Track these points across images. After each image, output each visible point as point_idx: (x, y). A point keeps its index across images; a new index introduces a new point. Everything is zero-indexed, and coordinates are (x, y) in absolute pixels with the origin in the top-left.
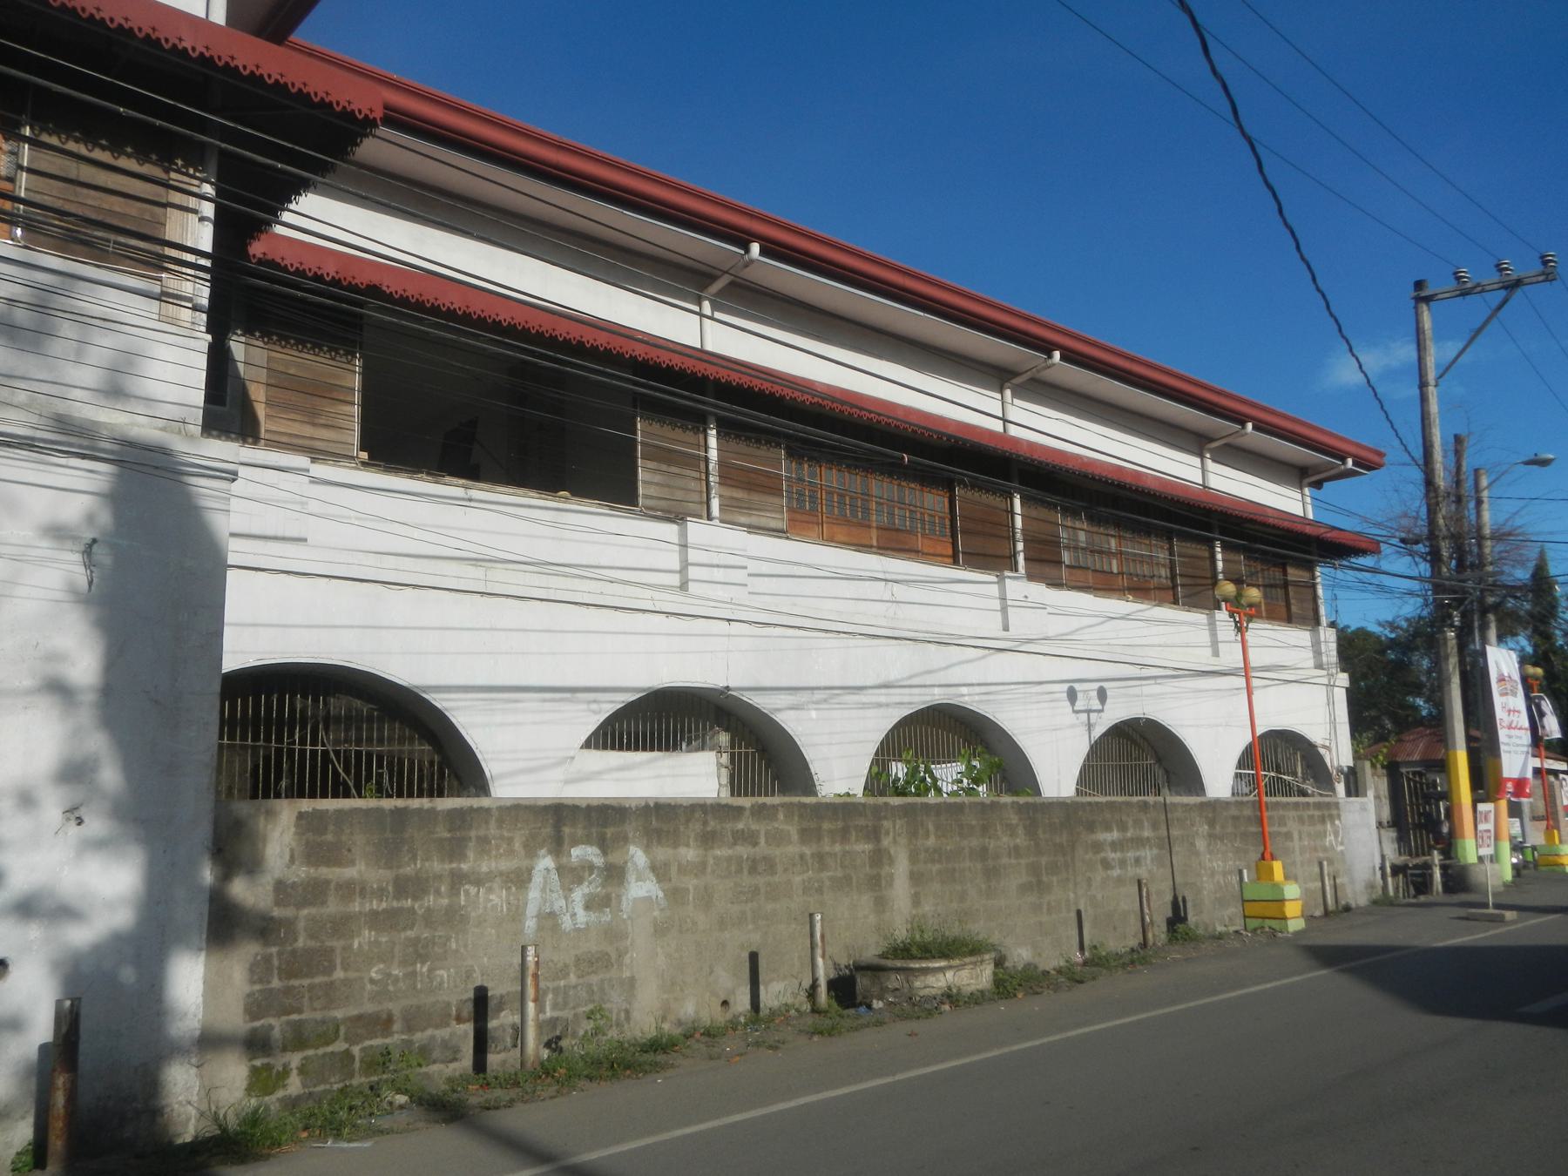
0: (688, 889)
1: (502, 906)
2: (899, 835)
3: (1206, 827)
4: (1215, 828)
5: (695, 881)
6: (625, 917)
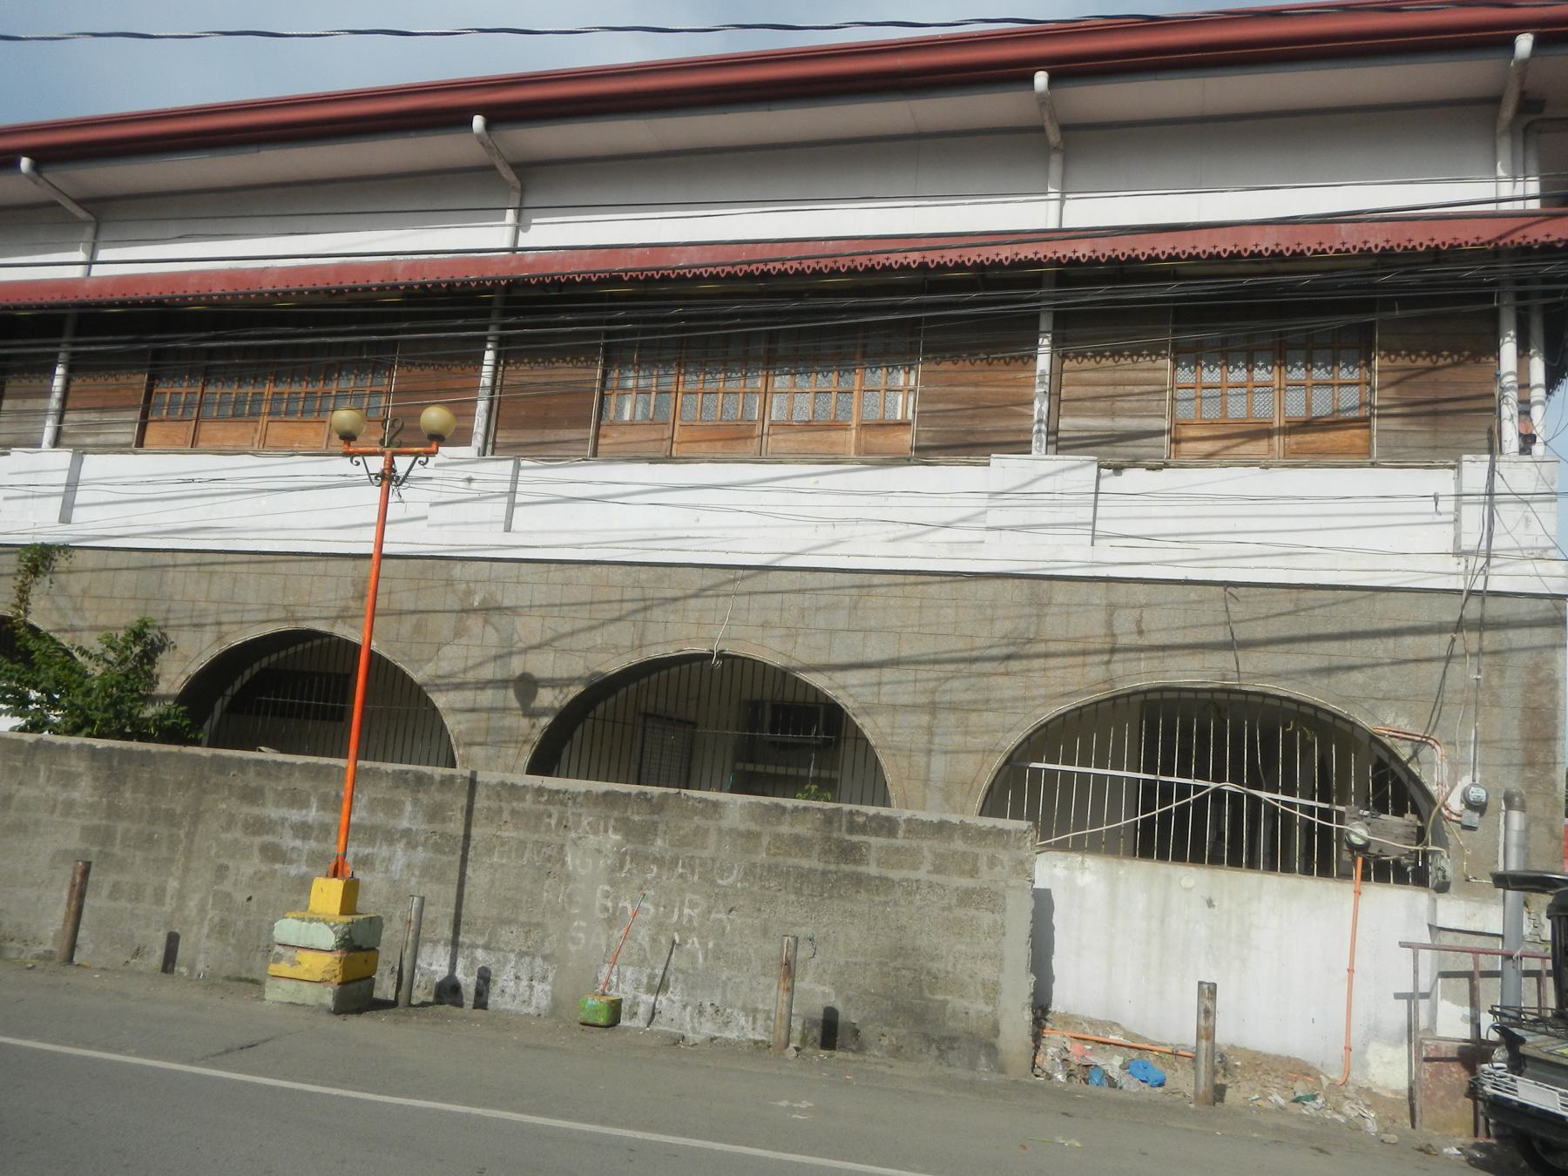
3: (616, 837)
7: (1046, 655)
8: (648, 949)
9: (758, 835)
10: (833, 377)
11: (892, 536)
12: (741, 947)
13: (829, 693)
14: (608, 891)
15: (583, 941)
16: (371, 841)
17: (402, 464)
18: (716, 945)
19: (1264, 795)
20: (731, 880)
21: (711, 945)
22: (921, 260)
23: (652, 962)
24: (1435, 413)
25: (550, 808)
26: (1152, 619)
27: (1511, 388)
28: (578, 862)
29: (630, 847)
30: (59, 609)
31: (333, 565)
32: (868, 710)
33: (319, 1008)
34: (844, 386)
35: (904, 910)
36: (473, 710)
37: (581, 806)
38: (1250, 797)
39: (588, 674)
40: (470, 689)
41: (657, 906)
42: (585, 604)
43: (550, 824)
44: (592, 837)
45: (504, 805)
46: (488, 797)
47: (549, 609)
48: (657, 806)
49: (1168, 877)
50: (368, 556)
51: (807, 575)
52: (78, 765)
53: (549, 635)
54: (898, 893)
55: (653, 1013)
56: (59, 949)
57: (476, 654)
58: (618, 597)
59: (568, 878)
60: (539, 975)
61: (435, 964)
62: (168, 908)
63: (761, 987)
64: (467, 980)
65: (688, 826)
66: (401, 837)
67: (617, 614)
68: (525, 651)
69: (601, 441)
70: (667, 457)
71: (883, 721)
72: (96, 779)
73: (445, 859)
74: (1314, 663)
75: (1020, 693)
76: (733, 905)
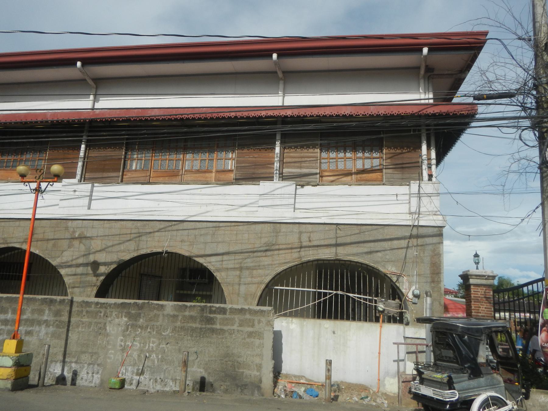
7: (279, 250)
8: (137, 360)
9: (177, 316)
10: (207, 154)
11: (227, 209)
12: (171, 357)
13: (205, 264)
14: (122, 339)
15: (113, 358)
16: (32, 325)
17: (43, 185)
18: (162, 357)
19: (351, 295)
20: (167, 333)
21: (160, 357)
22: (235, 115)
23: (138, 364)
24: (403, 168)
25: (101, 310)
26: (314, 236)
27: (425, 160)
28: (111, 329)
29: (131, 322)
31: (22, 223)
32: (218, 270)
33: (6, 389)
34: (210, 158)
35: (229, 340)
36: (75, 275)
37: (113, 308)
38: (347, 296)
39: (118, 260)
40: (74, 267)
41: (140, 343)
42: (118, 235)
43: (101, 316)
44: (116, 320)
45: (83, 309)
46: (78, 307)
47: (104, 237)
48: (140, 307)
49: (320, 324)
50: (30, 219)
51: (197, 223)
53: (104, 246)
54: (227, 334)
55: (139, 383)
57: (77, 254)
58: (130, 232)
59: (108, 335)
60: (95, 372)
61: (56, 370)
63: (178, 371)
64: (68, 375)
65: (152, 314)
66: (44, 323)
67: (129, 239)
68: (95, 253)
69: (124, 177)
70: (148, 182)
71: (223, 274)
73: (61, 330)
74: (366, 250)
75: (270, 263)
76: (168, 342)
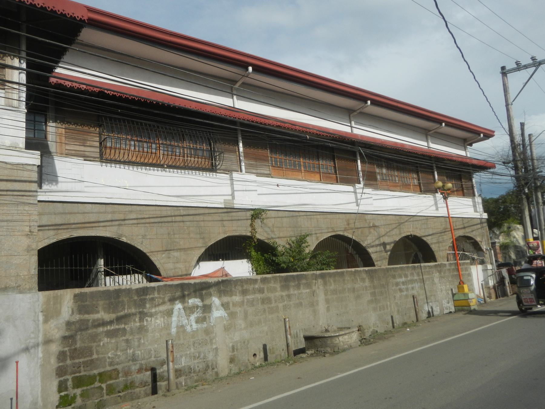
0: (237, 312)
1: (162, 324)
2: (320, 285)
3: (438, 274)
4: (441, 274)
5: (240, 309)
6: (212, 325)
30: (266, 232)
32: (432, 244)
36: (376, 252)
52: (364, 275)
56: (415, 319)
62: (389, 310)
72: (369, 279)
